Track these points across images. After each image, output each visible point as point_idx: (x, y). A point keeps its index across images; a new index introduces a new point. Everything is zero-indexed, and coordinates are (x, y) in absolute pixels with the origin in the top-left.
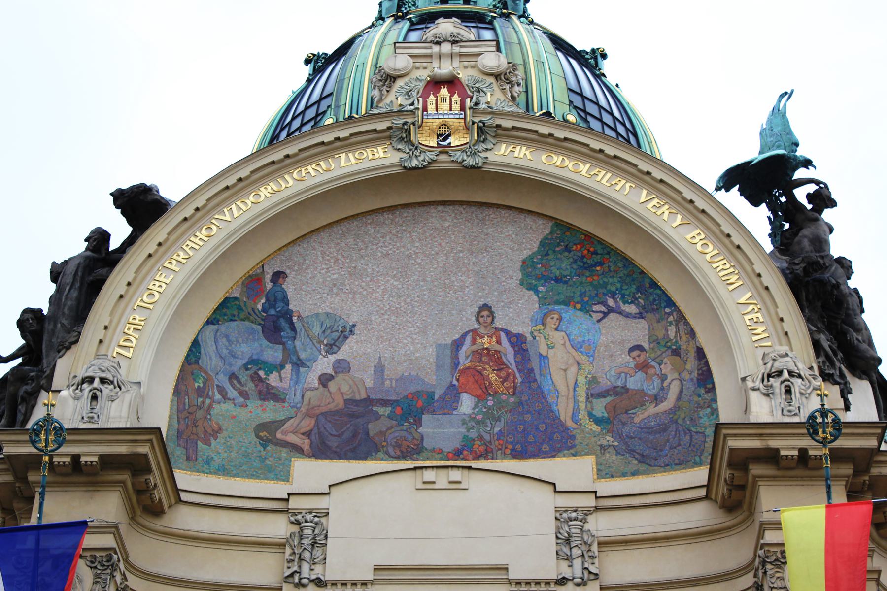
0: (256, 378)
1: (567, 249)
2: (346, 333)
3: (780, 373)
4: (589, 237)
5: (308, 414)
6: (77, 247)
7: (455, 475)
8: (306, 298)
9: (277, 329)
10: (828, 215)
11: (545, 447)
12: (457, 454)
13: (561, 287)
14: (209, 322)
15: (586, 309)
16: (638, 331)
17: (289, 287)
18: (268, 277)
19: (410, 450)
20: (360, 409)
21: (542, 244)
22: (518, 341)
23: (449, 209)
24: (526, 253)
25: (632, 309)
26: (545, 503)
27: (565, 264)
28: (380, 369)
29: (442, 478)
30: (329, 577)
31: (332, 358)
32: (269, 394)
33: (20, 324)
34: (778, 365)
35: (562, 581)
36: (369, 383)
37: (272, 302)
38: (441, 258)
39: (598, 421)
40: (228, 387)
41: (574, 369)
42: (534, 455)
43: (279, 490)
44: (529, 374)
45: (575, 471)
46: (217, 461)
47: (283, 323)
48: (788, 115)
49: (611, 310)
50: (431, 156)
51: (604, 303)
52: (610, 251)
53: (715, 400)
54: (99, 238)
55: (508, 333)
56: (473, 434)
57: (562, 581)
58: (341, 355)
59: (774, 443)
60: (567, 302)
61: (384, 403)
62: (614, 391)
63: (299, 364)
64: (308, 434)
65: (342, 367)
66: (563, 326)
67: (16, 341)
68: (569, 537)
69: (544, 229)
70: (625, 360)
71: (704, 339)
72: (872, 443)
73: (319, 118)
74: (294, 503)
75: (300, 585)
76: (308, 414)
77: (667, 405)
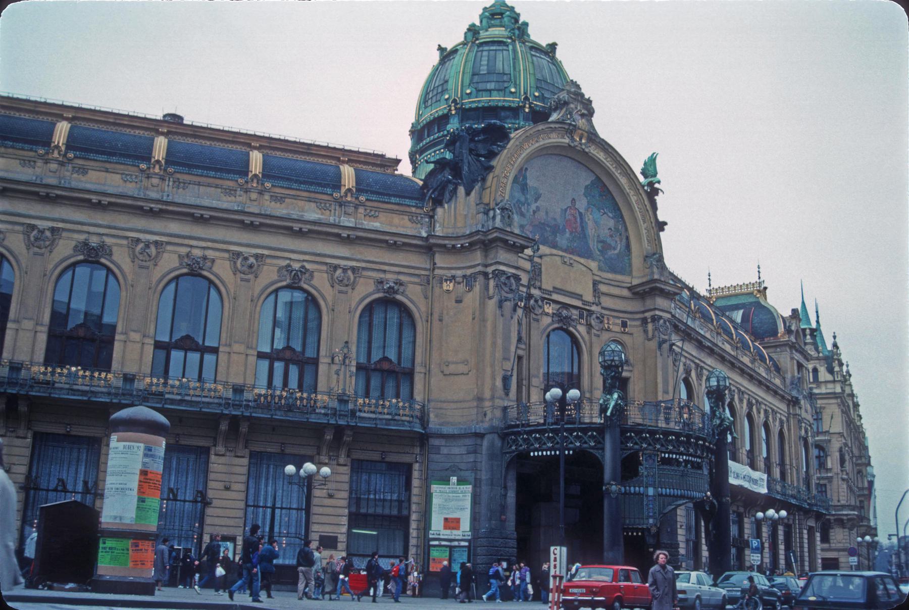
4: (605, 186)
15: (599, 210)
16: (611, 223)
19: (554, 246)
22: (580, 214)
25: (610, 215)
30: (544, 287)
45: (593, 265)
50: (576, 144)
61: (548, 226)
63: (528, 205)
65: (538, 208)
70: (607, 231)
73: (506, 85)
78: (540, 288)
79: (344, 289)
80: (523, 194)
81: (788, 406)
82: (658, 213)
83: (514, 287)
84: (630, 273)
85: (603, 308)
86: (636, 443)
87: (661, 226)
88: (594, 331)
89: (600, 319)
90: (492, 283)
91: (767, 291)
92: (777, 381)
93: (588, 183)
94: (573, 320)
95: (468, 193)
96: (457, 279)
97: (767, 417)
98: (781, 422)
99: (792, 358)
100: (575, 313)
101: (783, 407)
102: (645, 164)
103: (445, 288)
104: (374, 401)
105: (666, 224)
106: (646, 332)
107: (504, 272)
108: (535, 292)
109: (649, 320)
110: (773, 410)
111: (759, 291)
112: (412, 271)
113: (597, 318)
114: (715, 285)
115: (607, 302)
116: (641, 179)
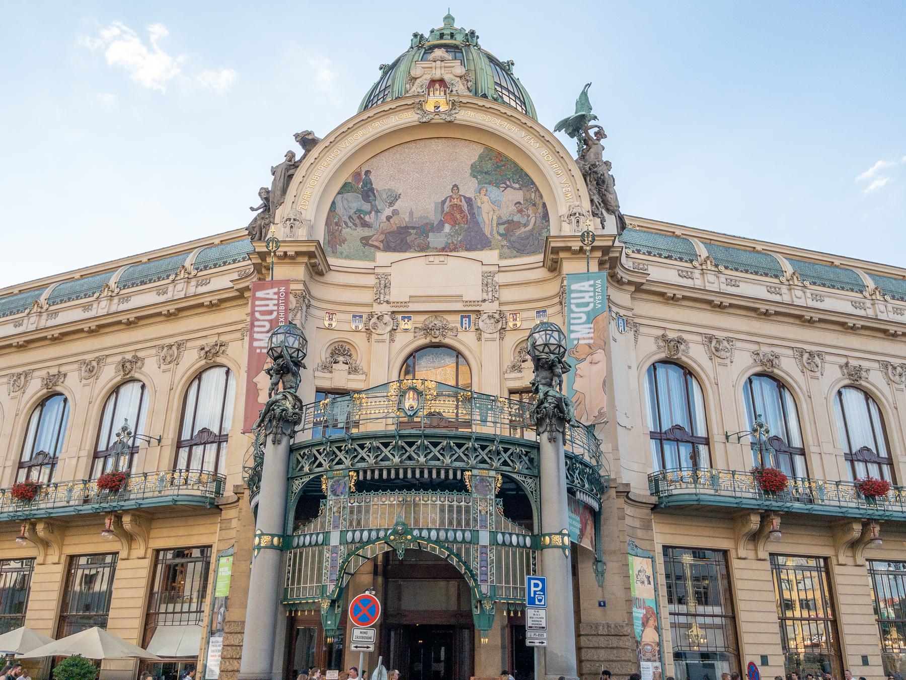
0: (360, 218)
1: (490, 159)
2: (397, 198)
3: (575, 214)
4: (500, 154)
5: (382, 233)
6: (283, 159)
7: (442, 258)
8: (380, 182)
9: (368, 196)
11: (479, 246)
12: (443, 249)
13: (487, 177)
14: (339, 193)
16: (519, 196)
17: (372, 177)
18: (363, 173)
19: (424, 248)
20: (404, 230)
21: (480, 157)
22: (469, 201)
23: (440, 141)
24: (473, 161)
25: (517, 186)
26: (478, 269)
27: (489, 166)
28: (411, 213)
29: (437, 260)
30: (391, 300)
31: (391, 209)
32: (365, 225)
33: (260, 194)
34: (575, 211)
35: (484, 301)
36: (407, 220)
37: (365, 185)
38: (437, 163)
39: (501, 235)
40: (348, 221)
41: (492, 213)
42: (474, 250)
43: (371, 265)
44: (473, 215)
45: (490, 256)
46: (345, 254)
47: (370, 193)
49: (508, 186)
51: (505, 183)
52: (508, 160)
53: (549, 225)
54: (291, 155)
55: (465, 197)
56: (450, 241)
57: (484, 301)
59: (569, 244)
60: (490, 183)
61: (413, 228)
62: (508, 222)
63: (377, 211)
64: (382, 242)
65: (395, 213)
66: (488, 193)
67: (258, 202)
68: (488, 282)
69: (480, 150)
70: (513, 208)
71: (546, 199)
72: (610, 243)
74: (377, 271)
75: (380, 303)
76: (382, 233)
78: (388, 302)
86: (320, 465)
88: (485, 336)
93: (474, 158)
94: (451, 330)
100: (453, 321)
108: (378, 309)
113: (491, 317)
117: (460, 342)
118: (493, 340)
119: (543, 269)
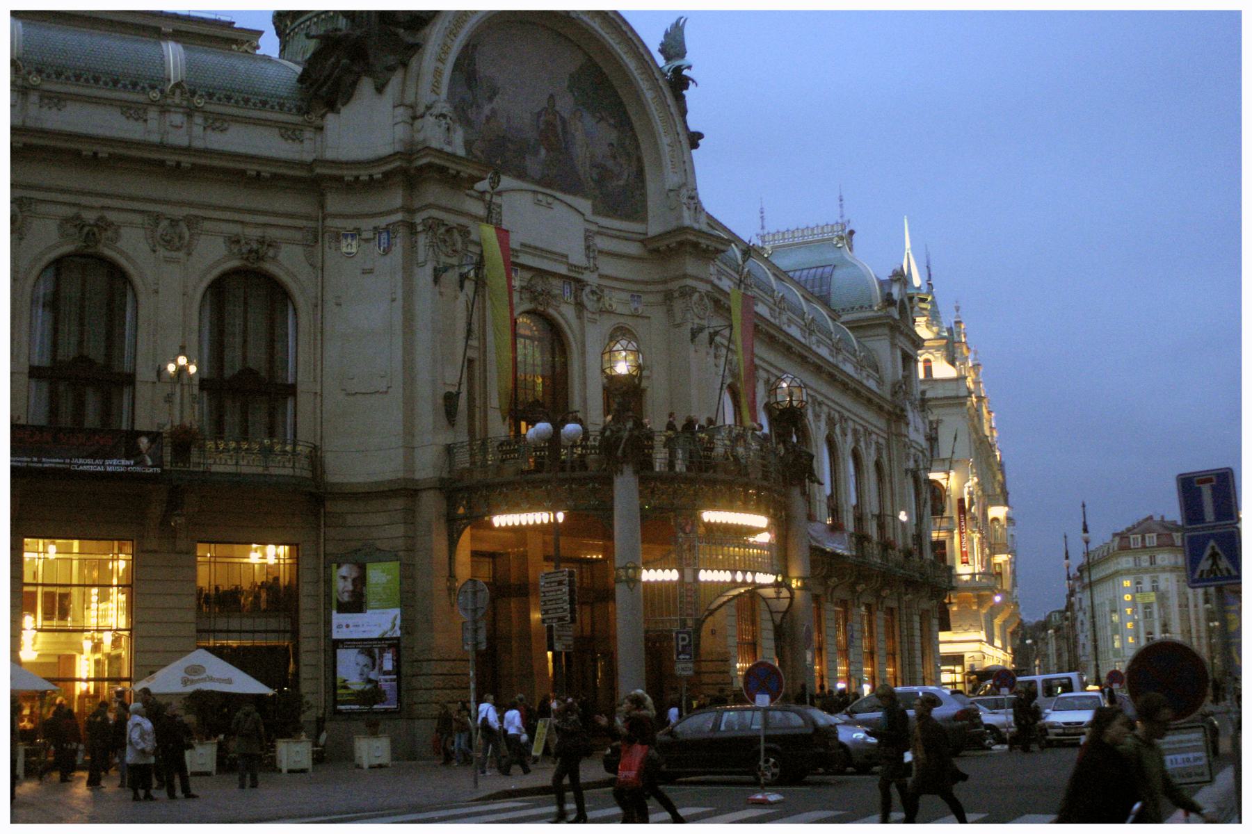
7: (550, 200)
10: (685, 92)
12: (538, 183)
15: (594, 116)
16: (613, 136)
19: (521, 175)
25: (612, 121)
31: (490, 106)
45: (585, 205)
48: (686, 32)
49: (601, 119)
57: (586, 268)
58: (494, 104)
59: (700, 240)
63: (478, 107)
64: (482, 152)
77: (621, 183)
79: (174, 254)
80: (470, 87)
81: (889, 422)
82: (688, 117)
83: (459, 246)
84: (644, 220)
85: (601, 276)
87: (695, 139)
88: (587, 314)
89: (598, 293)
90: (422, 240)
91: (854, 236)
92: (872, 384)
95: (380, 89)
96: (365, 235)
97: (857, 441)
98: (879, 450)
99: (893, 345)
100: (556, 286)
101: (882, 424)
102: (667, 35)
103: (344, 250)
104: (233, 445)
105: (700, 136)
106: (670, 312)
107: (441, 223)
109: (676, 295)
110: (866, 430)
111: (841, 238)
112: (289, 222)
114: (771, 227)
115: (608, 267)
116: (660, 60)
117: (562, 315)
118: (594, 321)
119: (639, 244)
